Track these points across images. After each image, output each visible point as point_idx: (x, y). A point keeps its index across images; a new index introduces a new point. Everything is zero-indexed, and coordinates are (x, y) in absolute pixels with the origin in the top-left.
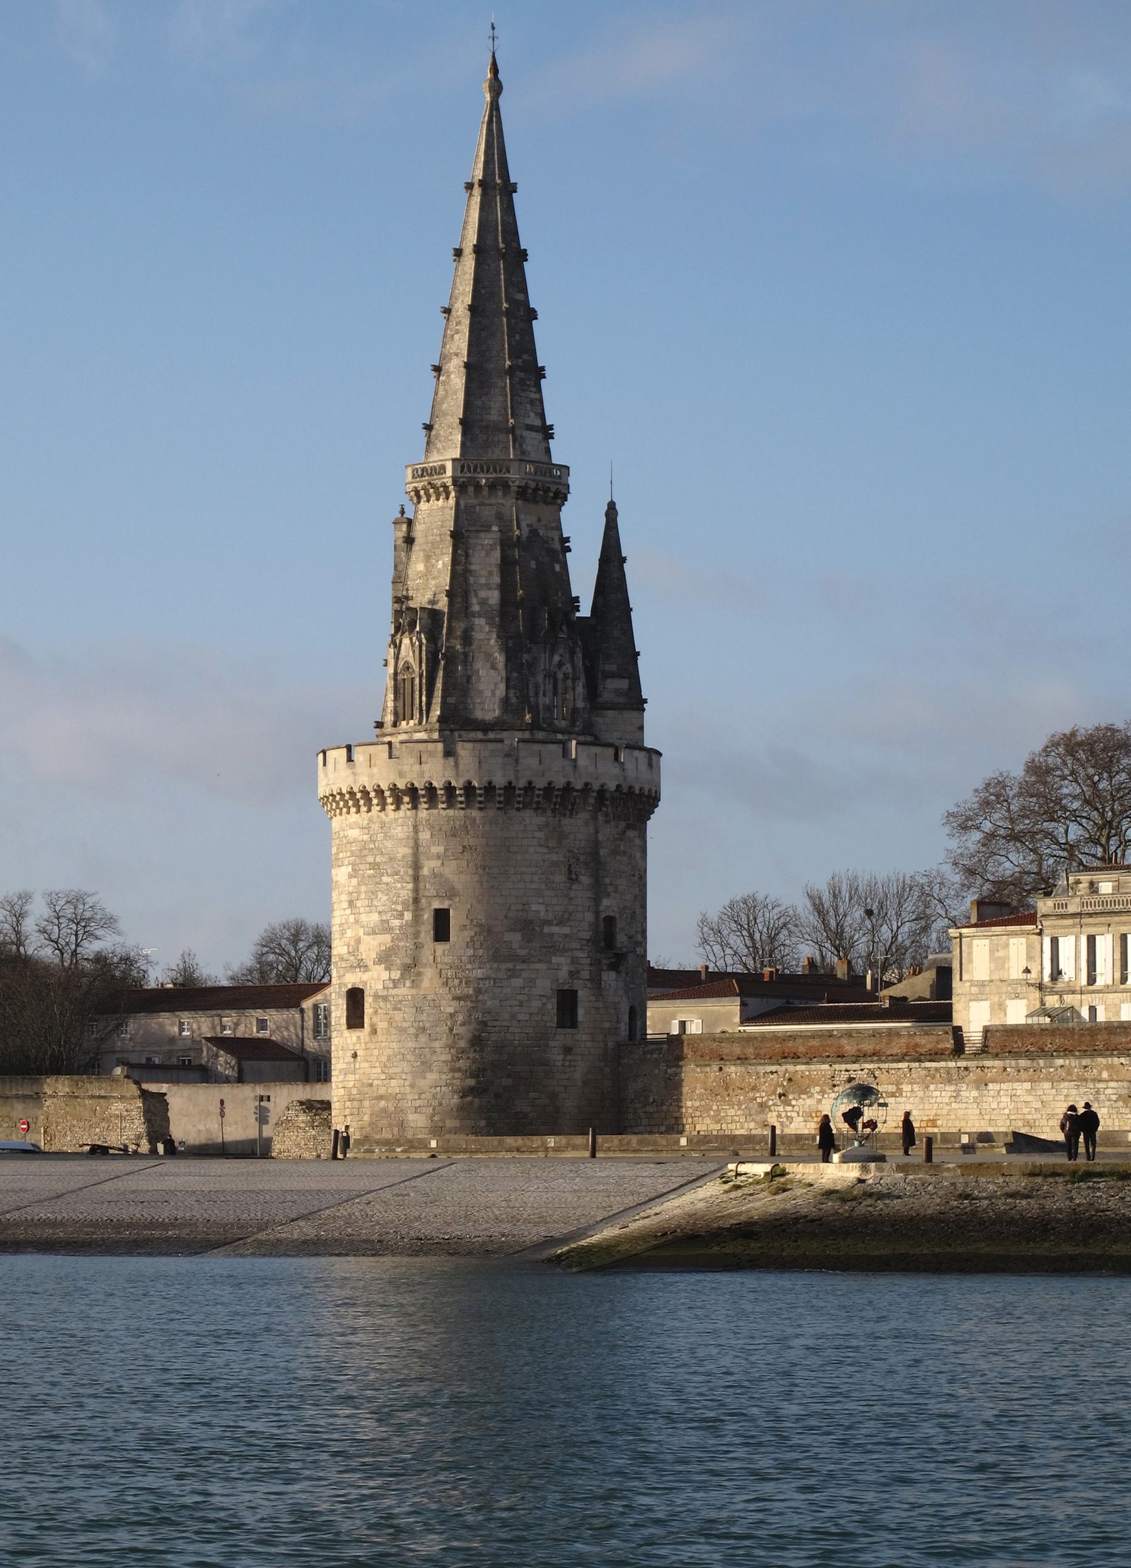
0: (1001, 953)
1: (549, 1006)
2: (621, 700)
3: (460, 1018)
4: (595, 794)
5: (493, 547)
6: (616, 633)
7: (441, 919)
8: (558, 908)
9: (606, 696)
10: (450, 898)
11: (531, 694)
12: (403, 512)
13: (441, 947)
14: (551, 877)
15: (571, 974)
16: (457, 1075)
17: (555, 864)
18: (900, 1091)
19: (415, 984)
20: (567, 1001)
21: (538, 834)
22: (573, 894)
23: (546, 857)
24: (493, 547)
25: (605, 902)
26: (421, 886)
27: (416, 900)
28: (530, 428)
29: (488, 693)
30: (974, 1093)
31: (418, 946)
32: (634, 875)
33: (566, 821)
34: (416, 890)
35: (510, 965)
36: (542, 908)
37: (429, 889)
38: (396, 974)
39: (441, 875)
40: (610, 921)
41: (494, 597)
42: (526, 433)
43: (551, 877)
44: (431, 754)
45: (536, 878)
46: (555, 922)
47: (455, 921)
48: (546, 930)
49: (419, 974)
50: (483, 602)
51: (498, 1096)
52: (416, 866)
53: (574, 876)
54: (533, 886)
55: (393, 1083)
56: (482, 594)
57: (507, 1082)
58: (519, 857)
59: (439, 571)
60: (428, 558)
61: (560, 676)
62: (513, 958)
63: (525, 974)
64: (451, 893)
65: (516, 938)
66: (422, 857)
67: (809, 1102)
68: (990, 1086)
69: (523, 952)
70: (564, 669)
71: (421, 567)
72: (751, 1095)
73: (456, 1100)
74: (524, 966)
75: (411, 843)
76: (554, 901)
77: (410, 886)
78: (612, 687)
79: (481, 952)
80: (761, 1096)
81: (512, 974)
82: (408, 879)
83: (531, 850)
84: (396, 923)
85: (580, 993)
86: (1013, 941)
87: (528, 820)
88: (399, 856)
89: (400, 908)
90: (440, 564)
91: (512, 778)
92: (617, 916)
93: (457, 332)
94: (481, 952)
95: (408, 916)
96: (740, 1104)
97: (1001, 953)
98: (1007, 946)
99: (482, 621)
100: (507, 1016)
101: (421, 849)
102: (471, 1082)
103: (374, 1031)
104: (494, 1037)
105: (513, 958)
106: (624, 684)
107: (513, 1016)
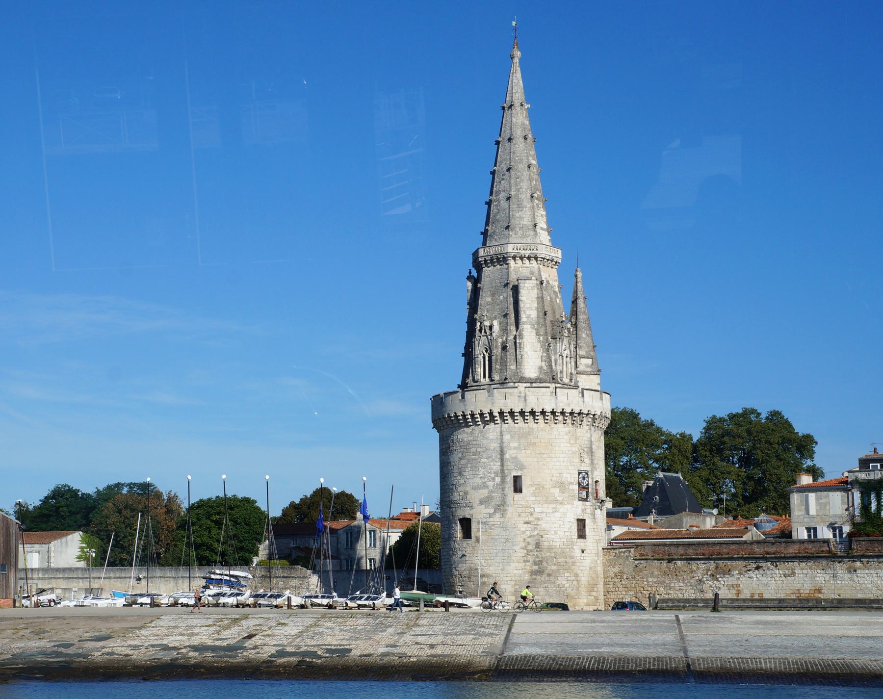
0: (824, 500)
2: (589, 369)
3: (528, 533)
5: (532, 288)
6: (584, 335)
7: (517, 479)
9: (581, 368)
10: (521, 470)
11: (553, 364)
12: (470, 273)
13: (518, 496)
15: (583, 510)
16: (528, 564)
17: (574, 452)
18: (793, 574)
19: (503, 516)
20: (581, 523)
21: (566, 437)
24: (532, 288)
25: (595, 473)
26: (505, 463)
27: (502, 471)
28: (542, 229)
29: (532, 364)
30: (849, 575)
31: (504, 496)
33: (579, 430)
34: (502, 465)
35: (554, 506)
36: (569, 476)
37: (509, 465)
38: (492, 511)
39: (516, 458)
41: (534, 314)
42: (541, 231)
44: (511, 394)
47: (525, 483)
48: (571, 487)
49: (505, 510)
50: (528, 317)
51: (549, 575)
52: (502, 453)
54: (565, 464)
55: (491, 568)
56: (528, 312)
57: (554, 568)
58: (557, 448)
59: (501, 301)
60: (493, 295)
61: (565, 355)
62: (555, 502)
64: (522, 467)
65: (556, 491)
66: (505, 449)
67: (731, 579)
68: (859, 571)
69: (560, 499)
70: (566, 352)
71: (489, 299)
72: (691, 575)
73: (527, 577)
74: (561, 506)
75: (499, 441)
77: (499, 464)
78: (585, 363)
79: (538, 499)
80: (699, 575)
81: (555, 510)
82: (497, 460)
84: (491, 483)
85: (588, 522)
86: (831, 493)
88: (492, 448)
89: (493, 475)
90: (501, 298)
91: (554, 407)
93: (503, 179)
94: (538, 499)
95: (498, 480)
96: (684, 580)
97: (824, 500)
98: (828, 496)
99: (529, 326)
100: (553, 532)
101: (505, 445)
102: (536, 567)
103: (478, 540)
104: (546, 544)
105: (555, 502)
106: (589, 361)
107: (556, 533)
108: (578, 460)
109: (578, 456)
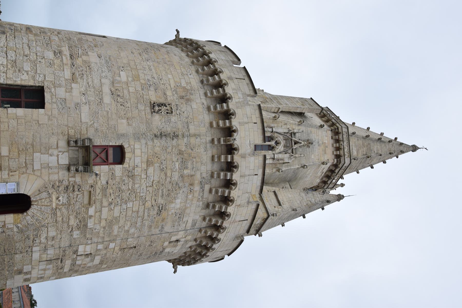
1: (25, 77)
4: (228, 124)
8: (126, 92)
14: (152, 88)
22: (141, 107)
23: (169, 87)
32: (162, 196)
40: (119, 155)
43: (152, 88)
45: (149, 77)
46: (113, 89)
53: (157, 108)
54: (142, 75)
61: (273, 143)
63: (57, 62)
76: (131, 89)
83: (170, 76)
87: (192, 76)
92: (126, 165)
108: (154, 99)
109: (162, 101)
